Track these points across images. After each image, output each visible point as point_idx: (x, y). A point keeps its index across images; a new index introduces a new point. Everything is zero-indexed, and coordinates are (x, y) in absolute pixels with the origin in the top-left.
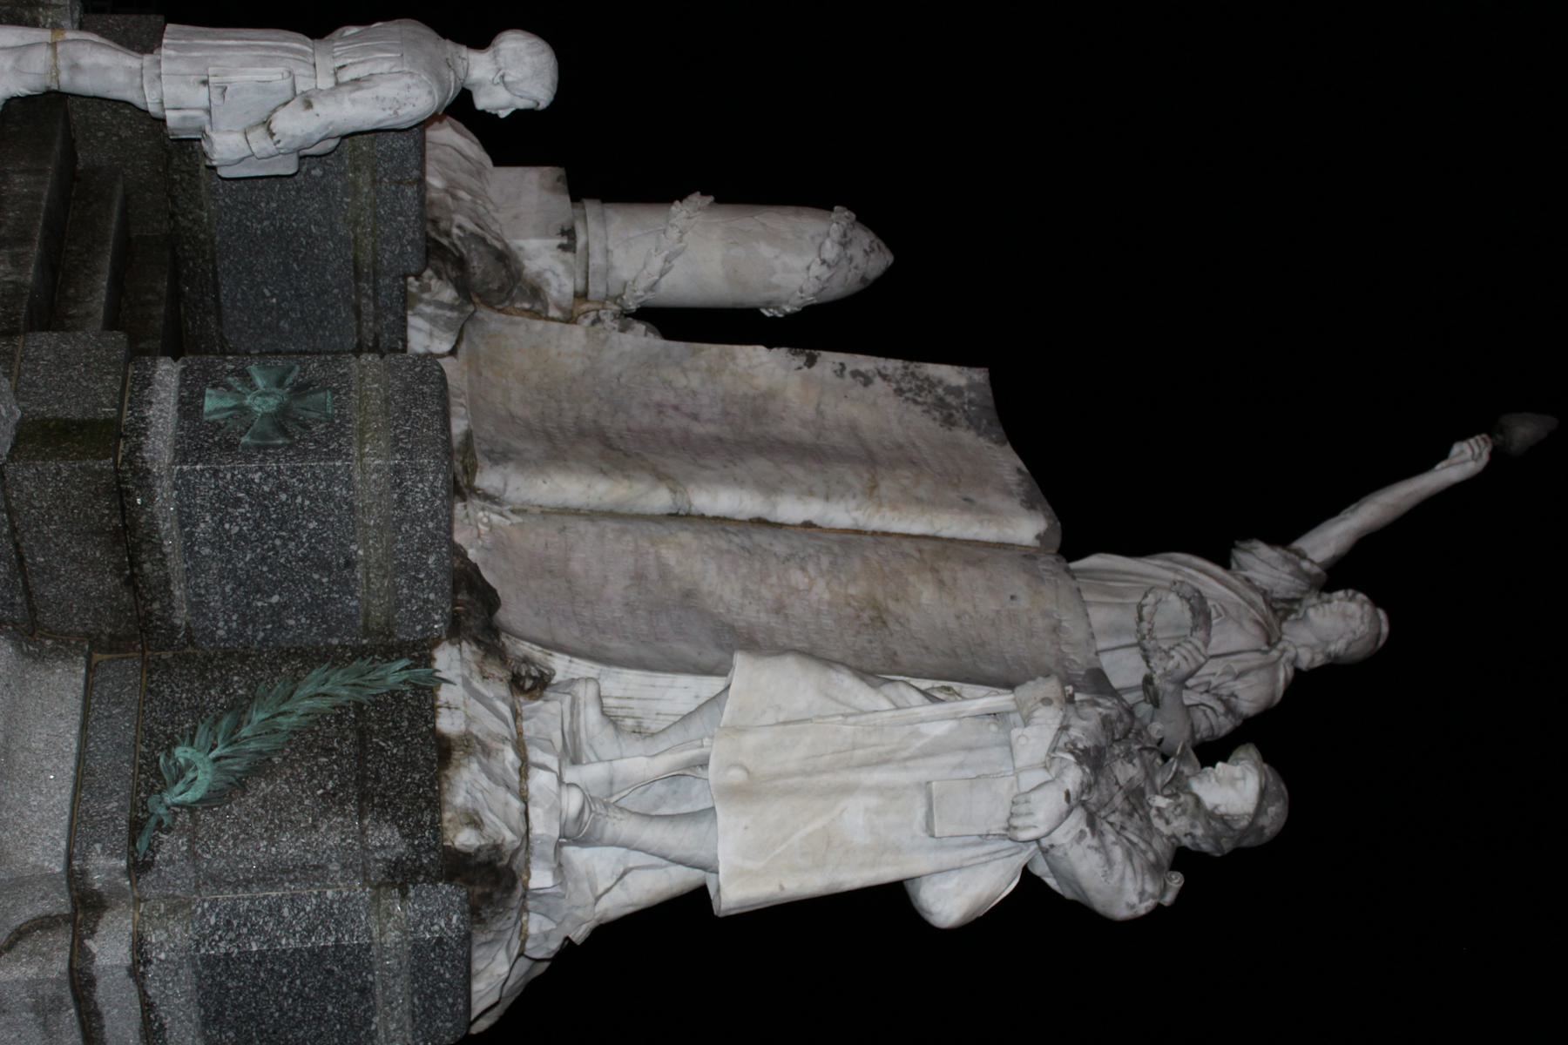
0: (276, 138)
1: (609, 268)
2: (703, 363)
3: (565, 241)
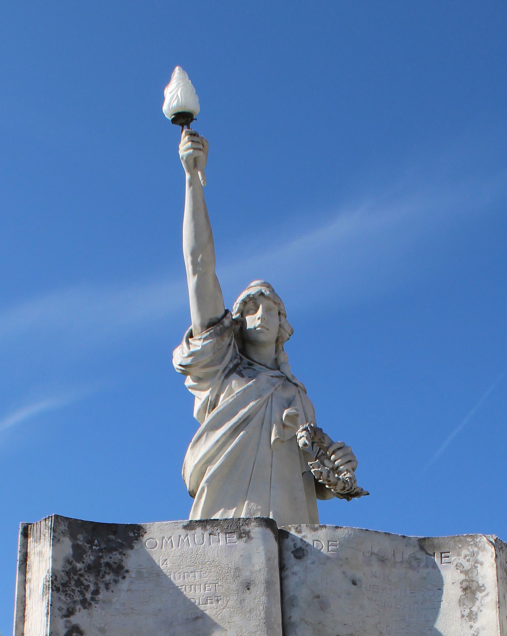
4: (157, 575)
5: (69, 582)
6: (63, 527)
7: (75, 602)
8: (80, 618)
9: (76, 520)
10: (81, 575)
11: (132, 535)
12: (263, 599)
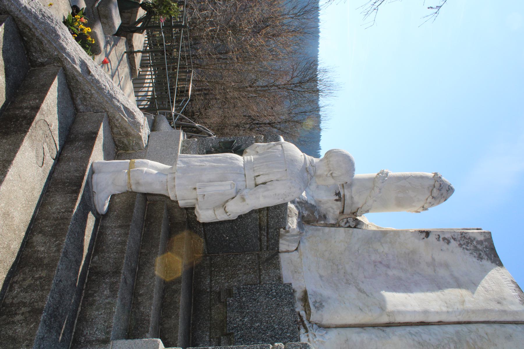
0: (228, 214)
1: (353, 203)
3: (337, 198)
4: (486, 271)
5: (467, 239)
6: (487, 236)
8: (453, 243)
9: (492, 241)
11: (497, 263)
12: (497, 309)
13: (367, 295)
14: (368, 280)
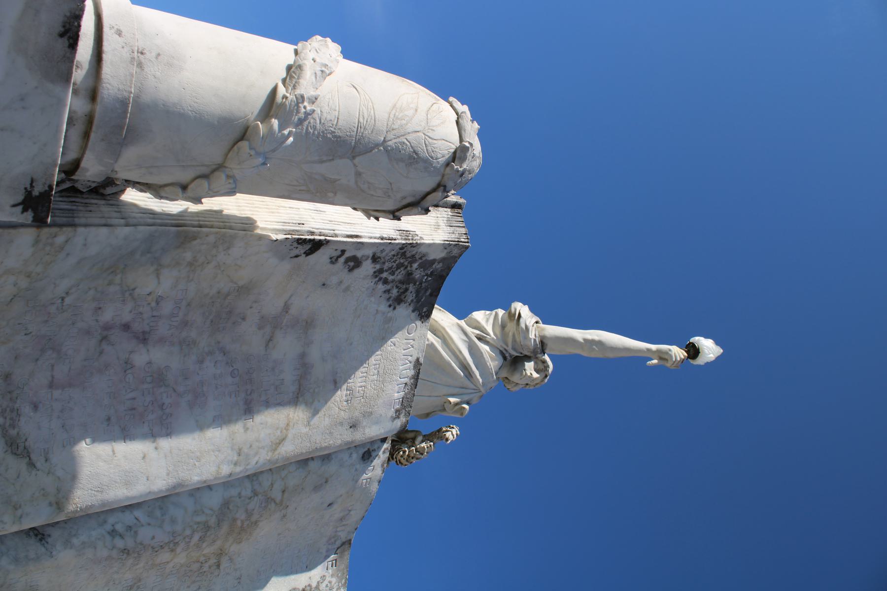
2: (188, 256)
7: (384, 263)
10: (406, 268)
11: (425, 310)
13: (32, 465)
14: (57, 393)
